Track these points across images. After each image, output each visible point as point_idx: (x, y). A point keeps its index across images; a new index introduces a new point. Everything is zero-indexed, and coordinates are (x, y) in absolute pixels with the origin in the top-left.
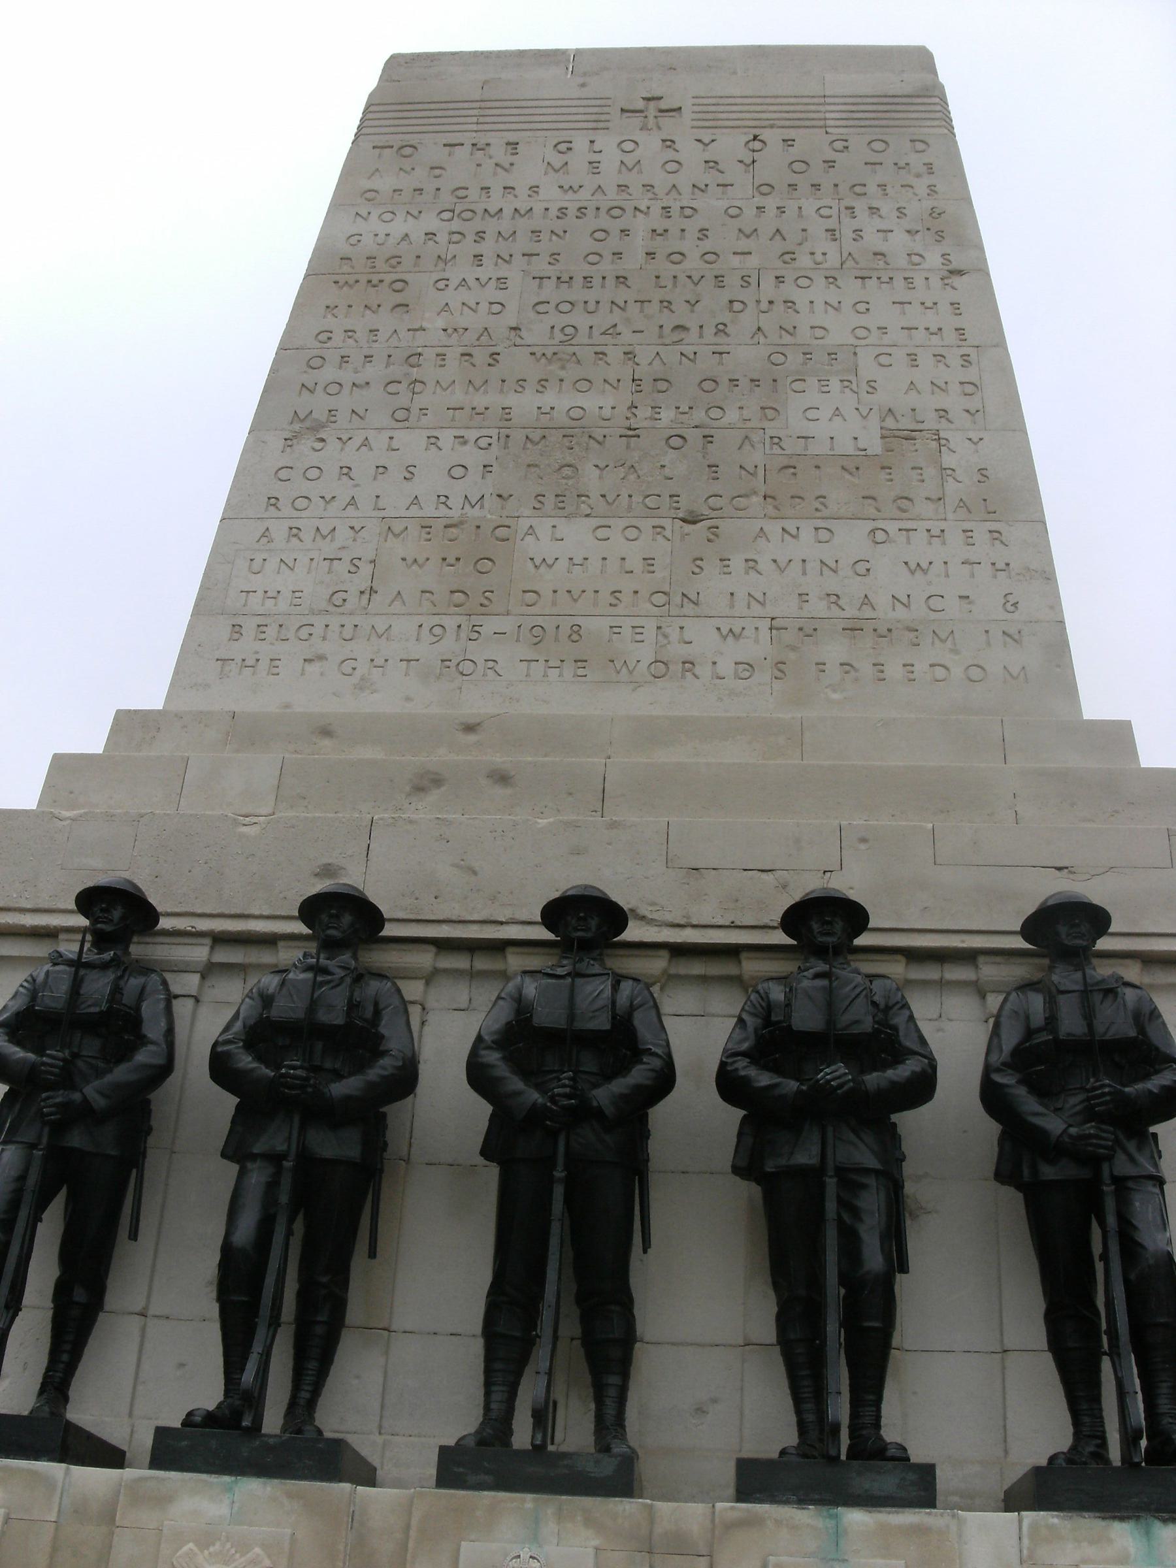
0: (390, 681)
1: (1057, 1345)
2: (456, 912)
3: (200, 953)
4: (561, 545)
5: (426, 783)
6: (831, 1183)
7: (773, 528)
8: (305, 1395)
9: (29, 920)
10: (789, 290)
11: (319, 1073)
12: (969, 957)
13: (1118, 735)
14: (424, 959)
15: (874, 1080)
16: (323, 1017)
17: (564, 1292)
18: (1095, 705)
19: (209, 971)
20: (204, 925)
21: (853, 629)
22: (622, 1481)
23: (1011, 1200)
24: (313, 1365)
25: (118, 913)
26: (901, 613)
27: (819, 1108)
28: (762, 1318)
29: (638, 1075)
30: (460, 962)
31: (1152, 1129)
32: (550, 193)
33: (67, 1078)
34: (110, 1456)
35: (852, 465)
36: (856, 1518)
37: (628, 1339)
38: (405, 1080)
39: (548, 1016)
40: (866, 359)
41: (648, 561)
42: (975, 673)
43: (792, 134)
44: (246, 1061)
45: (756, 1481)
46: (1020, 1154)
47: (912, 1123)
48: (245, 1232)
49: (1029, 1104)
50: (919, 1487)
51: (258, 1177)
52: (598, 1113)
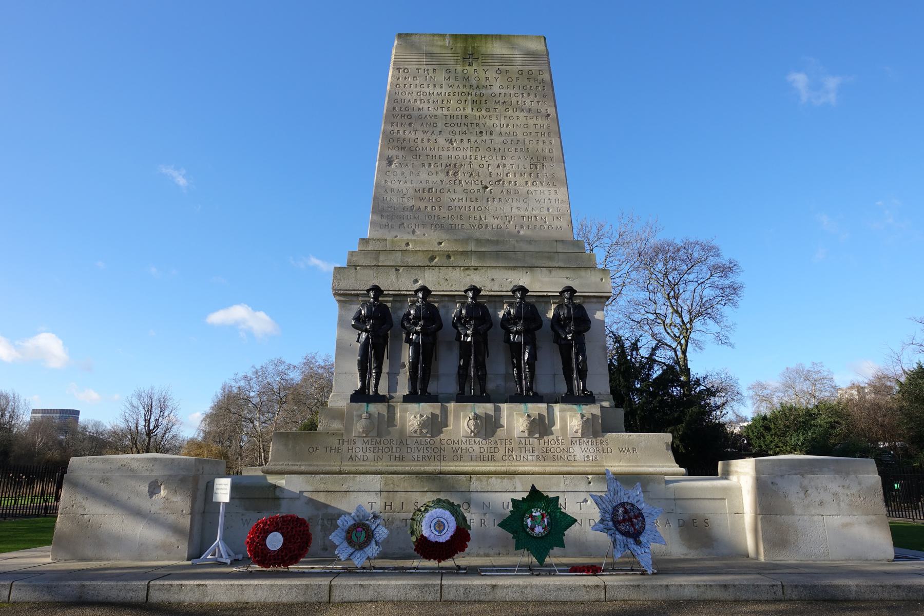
9: (353, 292)
12: (547, 296)
26: (534, 212)
30: (446, 299)
38: (440, 327)
43: (507, 68)
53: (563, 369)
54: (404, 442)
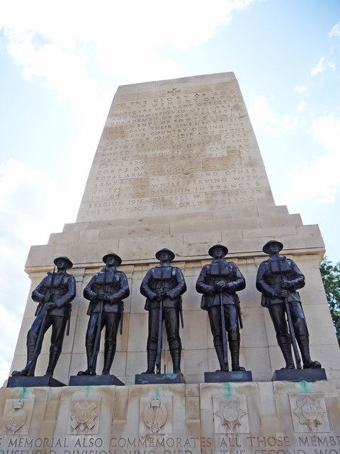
1: (280, 343)
2: (138, 258)
4: (158, 182)
5: (131, 232)
6: (222, 308)
7: (205, 174)
8: (107, 367)
10: (205, 125)
13: (284, 208)
14: (132, 268)
15: (230, 284)
16: (108, 281)
18: (278, 203)
20: (82, 266)
21: (224, 193)
22: (180, 380)
24: (108, 360)
25: (63, 263)
27: (217, 291)
29: (179, 288)
31: (297, 291)
32: (154, 111)
33: (51, 299)
34: (61, 385)
35: (222, 158)
36: (233, 385)
37: (180, 348)
38: (127, 294)
40: (223, 136)
41: (178, 183)
42: (251, 199)
45: (209, 377)
46: (267, 300)
49: (266, 287)
50: (248, 377)
52: (170, 297)
53: (278, 336)
54: (62, 443)
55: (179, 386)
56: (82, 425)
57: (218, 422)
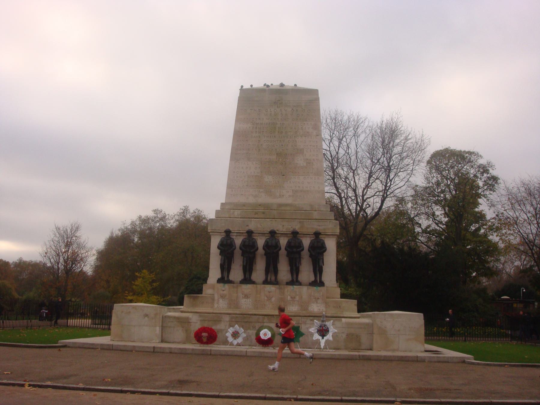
0: (250, 197)
3: (235, 234)
4: (268, 179)
11: (249, 248)
12: (309, 234)
14: (257, 235)
17: (272, 267)
19: (236, 236)
23: (311, 260)
25: (228, 232)
28: (289, 268)
36: (295, 286)
39: (270, 244)
44: (243, 248)
45: (288, 284)
46: (311, 256)
47: (302, 253)
48: (245, 264)
51: (245, 259)
55: (277, 286)
56: (246, 296)
57: (289, 297)
